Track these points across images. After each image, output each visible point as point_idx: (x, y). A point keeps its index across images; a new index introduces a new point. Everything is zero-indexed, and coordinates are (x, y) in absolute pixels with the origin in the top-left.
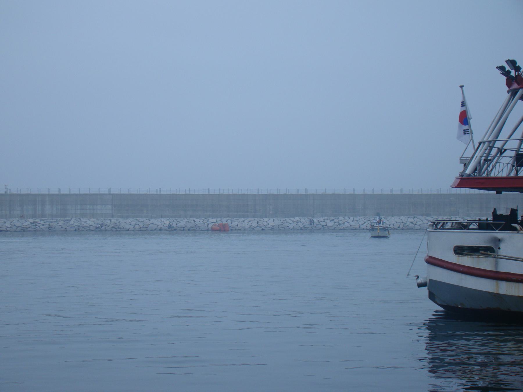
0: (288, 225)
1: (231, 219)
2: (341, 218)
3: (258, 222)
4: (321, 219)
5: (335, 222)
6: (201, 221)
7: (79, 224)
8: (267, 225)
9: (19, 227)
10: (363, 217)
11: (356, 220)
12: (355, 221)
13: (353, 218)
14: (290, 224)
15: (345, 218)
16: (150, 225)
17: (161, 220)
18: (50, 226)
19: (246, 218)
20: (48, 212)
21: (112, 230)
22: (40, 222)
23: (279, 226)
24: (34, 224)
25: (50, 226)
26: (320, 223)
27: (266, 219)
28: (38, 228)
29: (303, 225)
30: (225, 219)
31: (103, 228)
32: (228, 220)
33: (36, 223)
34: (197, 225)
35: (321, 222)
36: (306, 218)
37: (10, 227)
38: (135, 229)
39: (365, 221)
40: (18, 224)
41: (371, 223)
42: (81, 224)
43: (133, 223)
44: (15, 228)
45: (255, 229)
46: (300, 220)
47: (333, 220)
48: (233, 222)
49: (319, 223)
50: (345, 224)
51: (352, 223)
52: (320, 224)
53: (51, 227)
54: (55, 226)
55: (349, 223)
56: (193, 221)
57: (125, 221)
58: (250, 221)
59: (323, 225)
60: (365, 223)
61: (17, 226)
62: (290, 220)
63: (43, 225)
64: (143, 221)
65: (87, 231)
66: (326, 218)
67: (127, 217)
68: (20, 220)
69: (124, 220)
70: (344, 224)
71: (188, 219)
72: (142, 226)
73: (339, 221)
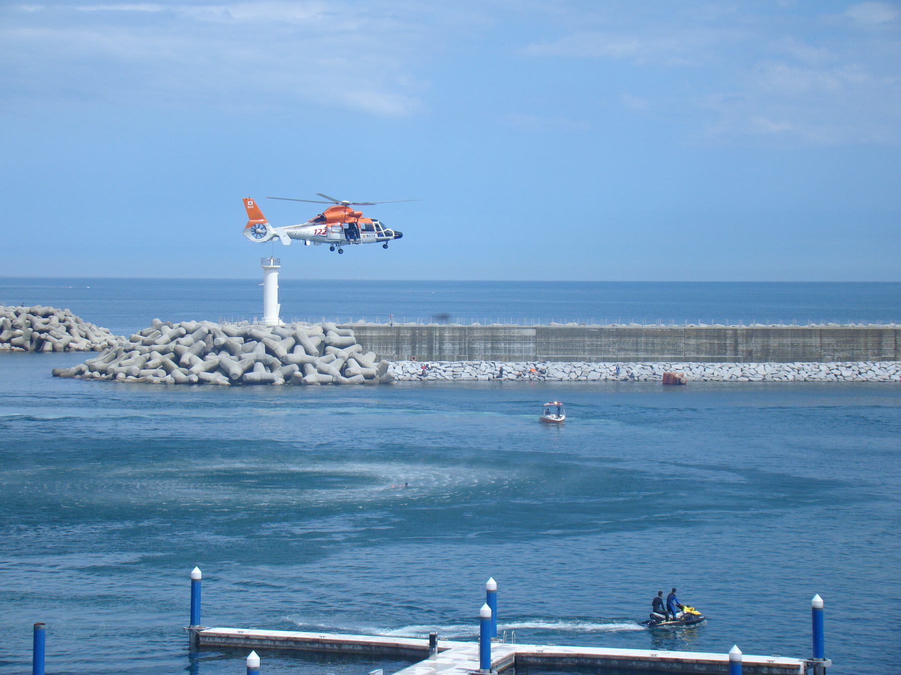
0: (786, 375)
1: (702, 364)
2: (861, 364)
3: (741, 369)
4: (833, 365)
5: (853, 370)
6: (661, 367)
7: (493, 371)
8: (755, 374)
9: (413, 374)
10: (894, 362)
12: (882, 369)
13: (880, 364)
14: (788, 373)
15: (867, 363)
16: (590, 372)
17: (605, 365)
18: (454, 373)
19: (724, 364)
20: (447, 353)
21: (540, 380)
22: (440, 367)
24: (433, 370)
25: (454, 373)
26: (832, 371)
27: (753, 365)
28: (439, 376)
29: (807, 375)
30: (694, 363)
31: (527, 376)
33: (435, 369)
34: (656, 373)
35: (833, 369)
36: (810, 363)
37: (402, 374)
38: (571, 378)
39: (898, 369)
40: (412, 370)
42: (496, 370)
43: (567, 370)
45: (739, 379)
47: (850, 367)
48: (707, 369)
50: (868, 373)
51: (878, 372)
52: (832, 373)
55: (874, 371)
56: (649, 368)
57: (555, 367)
58: (730, 368)
60: (897, 371)
62: (788, 366)
63: (445, 371)
64: (580, 367)
65: (504, 380)
66: (839, 363)
67: (556, 360)
69: (554, 365)
70: (866, 373)
71: (642, 365)
72: (579, 375)
73: (859, 368)
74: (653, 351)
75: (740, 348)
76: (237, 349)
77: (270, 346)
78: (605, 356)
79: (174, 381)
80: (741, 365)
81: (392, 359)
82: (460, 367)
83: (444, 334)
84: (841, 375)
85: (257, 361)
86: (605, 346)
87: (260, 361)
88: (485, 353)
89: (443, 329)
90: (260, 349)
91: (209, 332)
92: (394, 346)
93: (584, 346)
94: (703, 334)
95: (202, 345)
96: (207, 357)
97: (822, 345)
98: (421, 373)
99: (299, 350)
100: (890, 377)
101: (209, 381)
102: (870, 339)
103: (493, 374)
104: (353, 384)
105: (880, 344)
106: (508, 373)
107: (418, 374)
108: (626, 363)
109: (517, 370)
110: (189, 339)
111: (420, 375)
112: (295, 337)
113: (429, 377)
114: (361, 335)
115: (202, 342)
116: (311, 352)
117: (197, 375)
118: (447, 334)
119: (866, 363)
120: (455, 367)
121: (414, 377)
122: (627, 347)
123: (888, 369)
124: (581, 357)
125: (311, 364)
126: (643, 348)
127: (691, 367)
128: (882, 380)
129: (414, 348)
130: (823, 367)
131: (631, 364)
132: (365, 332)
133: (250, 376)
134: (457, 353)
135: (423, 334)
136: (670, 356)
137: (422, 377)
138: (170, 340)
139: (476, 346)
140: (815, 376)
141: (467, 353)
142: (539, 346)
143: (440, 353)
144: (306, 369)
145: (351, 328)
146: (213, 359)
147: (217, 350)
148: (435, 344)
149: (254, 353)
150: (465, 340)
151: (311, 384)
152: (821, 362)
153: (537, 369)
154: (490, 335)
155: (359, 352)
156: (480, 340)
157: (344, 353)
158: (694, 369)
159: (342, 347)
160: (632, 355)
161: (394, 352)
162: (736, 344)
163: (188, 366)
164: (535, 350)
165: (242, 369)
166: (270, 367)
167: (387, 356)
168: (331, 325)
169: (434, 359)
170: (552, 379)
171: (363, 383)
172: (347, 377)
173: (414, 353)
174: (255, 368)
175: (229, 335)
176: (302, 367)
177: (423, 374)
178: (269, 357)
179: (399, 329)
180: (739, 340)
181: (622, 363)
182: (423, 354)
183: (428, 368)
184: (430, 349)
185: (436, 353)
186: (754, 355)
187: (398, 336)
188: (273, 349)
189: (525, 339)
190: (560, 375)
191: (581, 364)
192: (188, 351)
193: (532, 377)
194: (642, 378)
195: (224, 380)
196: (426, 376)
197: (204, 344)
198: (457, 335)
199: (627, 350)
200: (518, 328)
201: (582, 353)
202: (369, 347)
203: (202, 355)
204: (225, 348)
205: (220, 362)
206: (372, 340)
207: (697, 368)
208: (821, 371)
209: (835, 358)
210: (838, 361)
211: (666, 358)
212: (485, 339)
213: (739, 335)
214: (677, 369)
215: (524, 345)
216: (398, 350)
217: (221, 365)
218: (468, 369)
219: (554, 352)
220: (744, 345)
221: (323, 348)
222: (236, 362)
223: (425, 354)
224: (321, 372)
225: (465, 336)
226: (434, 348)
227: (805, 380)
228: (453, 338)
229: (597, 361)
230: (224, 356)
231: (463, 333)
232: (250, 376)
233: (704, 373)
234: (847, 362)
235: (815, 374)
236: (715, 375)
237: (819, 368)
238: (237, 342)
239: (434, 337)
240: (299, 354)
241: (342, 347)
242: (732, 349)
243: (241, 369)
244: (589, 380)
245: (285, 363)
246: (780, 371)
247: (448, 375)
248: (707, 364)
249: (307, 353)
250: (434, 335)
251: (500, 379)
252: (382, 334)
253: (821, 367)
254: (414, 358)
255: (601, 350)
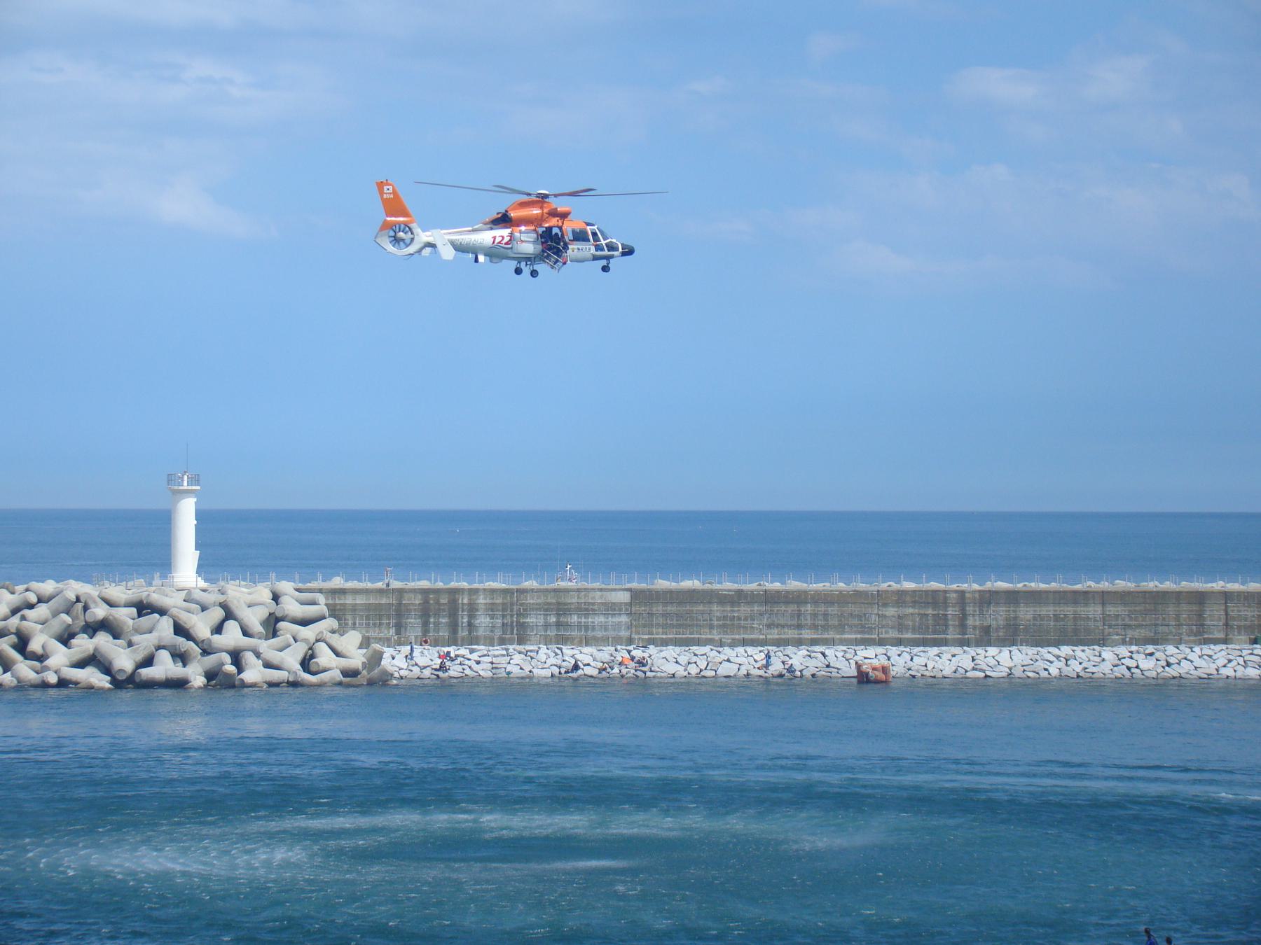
0: (1047, 667)
1: (908, 650)
2: (1171, 649)
3: (973, 657)
4: (1123, 651)
6: (840, 654)
7: (559, 662)
8: (995, 666)
9: (425, 667)
10: (1224, 647)
11: (1208, 656)
12: (1205, 657)
13: (1201, 649)
16: (721, 663)
17: (746, 652)
18: (494, 666)
19: (944, 648)
20: (481, 632)
22: (469, 656)
23: (1025, 667)
25: (494, 666)
26: (1123, 661)
27: (992, 651)
28: (468, 672)
29: (1081, 667)
30: (894, 648)
31: (616, 670)
32: (902, 652)
33: (462, 659)
34: (831, 665)
35: (1124, 658)
36: (1086, 648)
37: (405, 667)
38: (689, 674)
39: (1231, 657)
40: (422, 661)
41: (1245, 662)
42: (564, 661)
44: (416, 670)
45: (968, 674)
46: (1072, 653)
47: (1152, 654)
48: (915, 658)
49: (1119, 662)
51: (1198, 662)
52: (1123, 664)
53: (496, 668)
54: (505, 666)
55: (1192, 662)
56: (820, 655)
57: (663, 654)
58: (954, 656)
59: (1130, 666)
60: (1230, 661)
61: (420, 665)
62: (1049, 652)
63: (478, 663)
64: (705, 654)
66: (1134, 648)
67: (665, 643)
68: (425, 652)
69: (661, 651)
70: (1179, 664)
71: (808, 651)
74: (826, 628)
75: (970, 622)
76: (125, 628)
77: (183, 624)
78: (746, 636)
79: (15, 682)
80: (972, 651)
81: (388, 642)
82: (504, 655)
83: (476, 599)
84: (1137, 667)
85: (159, 648)
86: (746, 619)
87: (164, 647)
88: (546, 631)
89: (476, 591)
90: (165, 628)
91: (78, 600)
92: (393, 621)
93: (711, 620)
94: (908, 599)
95: (65, 622)
96: (74, 641)
97: (1105, 618)
98: (438, 667)
99: (232, 627)
100: (1217, 670)
101: (76, 683)
102: (1184, 607)
103: (560, 667)
104: (321, 685)
105: (1200, 616)
106: (585, 665)
107: (434, 667)
108: (782, 648)
109: (598, 660)
110: (42, 611)
111: (436, 670)
112: (224, 606)
113: (452, 673)
114: (337, 602)
115: (64, 617)
116: (251, 632)
117: (56, 672)
118: (481, 600)
119: (1178, 648)
120: (495, 656)
121: (427, 673)
122: (782, 622)
123: (1214, 658)
124: (706, 639)
125: (251, 653)
126: (809, 622)
127: (888, 654)
128: (1206, 676)
129: (425, 625)
130: (1108, 654)
131: (790, 650)
132: (343, 597)
133: (146, 673)
134: (498, 633)
135: (442, 601)
136: (854, 636)
137: (440, 674)
138: (9, 613)
139: (530, 620)
140: (1094, 670)
141: (515, 631)
142: (635, 620)
143: (470, 633)
144: (243, 661)
145: (320, 591)
146: (83, 644)
147: (91, 631)
148: (462, 618)
149: (155, 634)
150: (512, 611)
151: (253, 685)
152: (1104, 645)
153: (633, 658)
154: (554, 601)
155: (333, 632)
156: (537, 609)
157: (308, 633)
158: (895, 659)
159: (305, 622)
160: (791, 634)
161: (392, 631)
162: (963, 617)
163: (41, 658)
164: (629, 627)
165: (136, 662)
166: (181, 657)
167: (380, 639)
168: (286, 587)
169: (459, 643)
170: (659, 674)
171: (340, 684)
172: (314, 674)
173: (425, 631)
174: (155, 660)
175: (110, 604)
176: (236, 657)
177: (442, 668)
178: (181, 640)
179: (401, 592)
180: (968, 609)
181: (774, 648)
182: (441, 634)
183: (450, 657)
184: (454, 627)
185: (463, 633)
186: (994, 635)
187: (400, 604)
188: (187, 626)
189: (611, 608)
190: (671, 668)
191: (706, 649)
192: (42, 631)
193: (624, 671)
194: (807, 673)
195: (102, 681)
196: (446, 671)
197: (68, 619)
198: (498, 601)
199: (783, 626)
200: (601, 590)
201: (708, 631)
202: (350, 622)
203: (66, 639)
204: (104, 626)
205: (96, 649)
206: (355, 610)
207: (899, 655)
208: (1103, 660)
209: (1128, 639)
210: (1131, 644)
211: (848, 638)
212: (546, 608)
213: (967, 601)
214: (865, 658)
215: (610, 619)
216: (399, 627)
217: (96, 654)
218: (518, 658)
219: (660, 630)
220: (977, 618)
221: (272, 624)
222: (122, 650)
223: (444, 633)
224: (268, 665)
225: (512, 604)
226: (460, 624)
227: (1078, 676)
228: (491, 608)
229: (733, 644)
230: (102, 640)
231: (509, 598)
232: (146, 673)
233: (910, 664)
234: (1148, 646)
235: (1094, 666)
236: (930, 667)
237: (1100, 656)
238: (125, 615)
239: (460, 605)
240: (232, 636)
241: (305, 622)
242: (957, 623)
243: (132, 661)
244: (720, 677)
245: (205, 652)
246: (1037, 660)
247: (484, 671)
248: (916, 650)
249: (246, 633)
250: (460, 602)
251: (570, 675)
252: (372, 601)
253: (1104, 655)
254: (426, 642)
255: (739, 627)
